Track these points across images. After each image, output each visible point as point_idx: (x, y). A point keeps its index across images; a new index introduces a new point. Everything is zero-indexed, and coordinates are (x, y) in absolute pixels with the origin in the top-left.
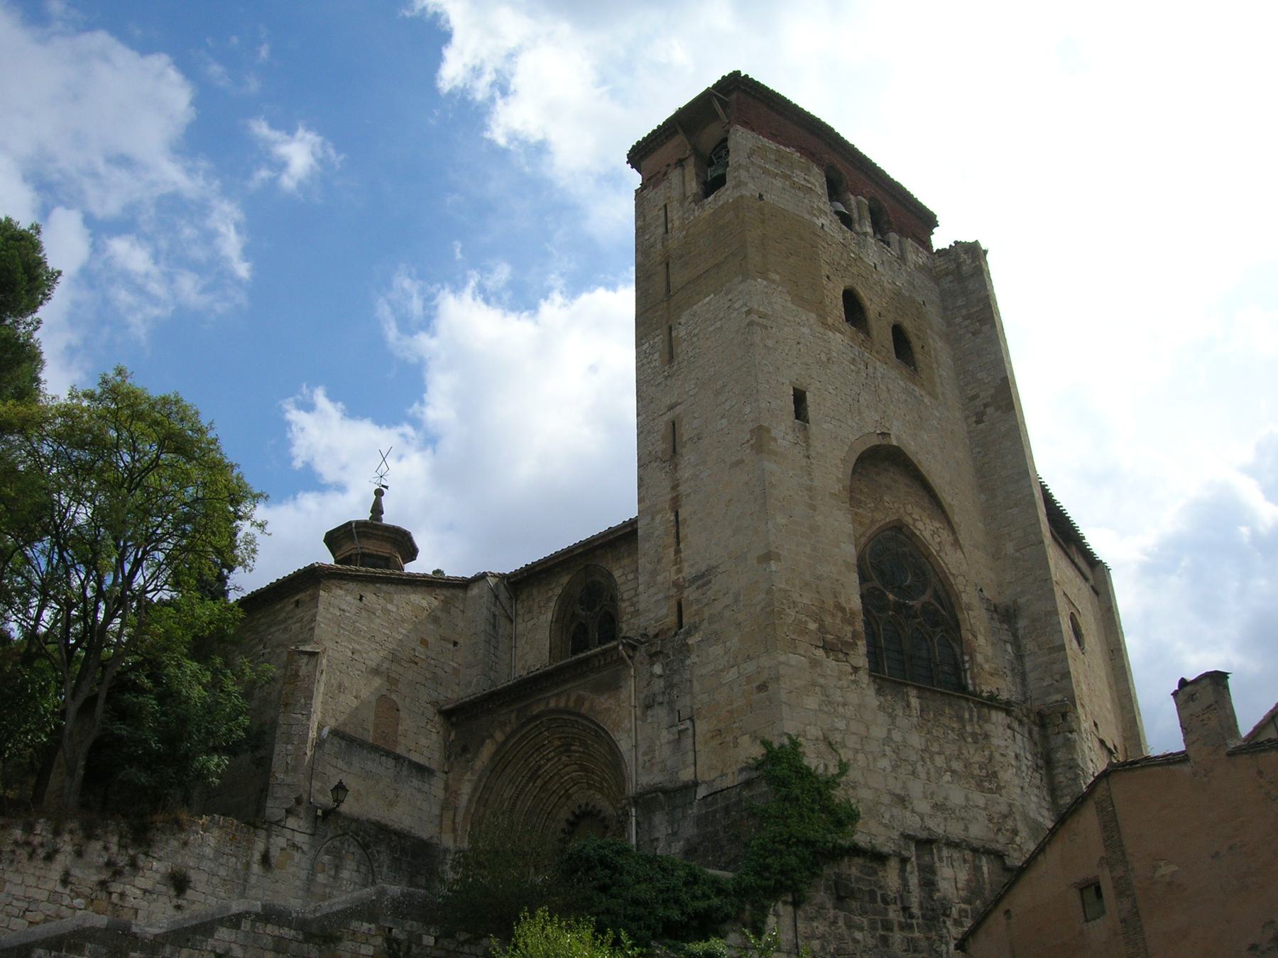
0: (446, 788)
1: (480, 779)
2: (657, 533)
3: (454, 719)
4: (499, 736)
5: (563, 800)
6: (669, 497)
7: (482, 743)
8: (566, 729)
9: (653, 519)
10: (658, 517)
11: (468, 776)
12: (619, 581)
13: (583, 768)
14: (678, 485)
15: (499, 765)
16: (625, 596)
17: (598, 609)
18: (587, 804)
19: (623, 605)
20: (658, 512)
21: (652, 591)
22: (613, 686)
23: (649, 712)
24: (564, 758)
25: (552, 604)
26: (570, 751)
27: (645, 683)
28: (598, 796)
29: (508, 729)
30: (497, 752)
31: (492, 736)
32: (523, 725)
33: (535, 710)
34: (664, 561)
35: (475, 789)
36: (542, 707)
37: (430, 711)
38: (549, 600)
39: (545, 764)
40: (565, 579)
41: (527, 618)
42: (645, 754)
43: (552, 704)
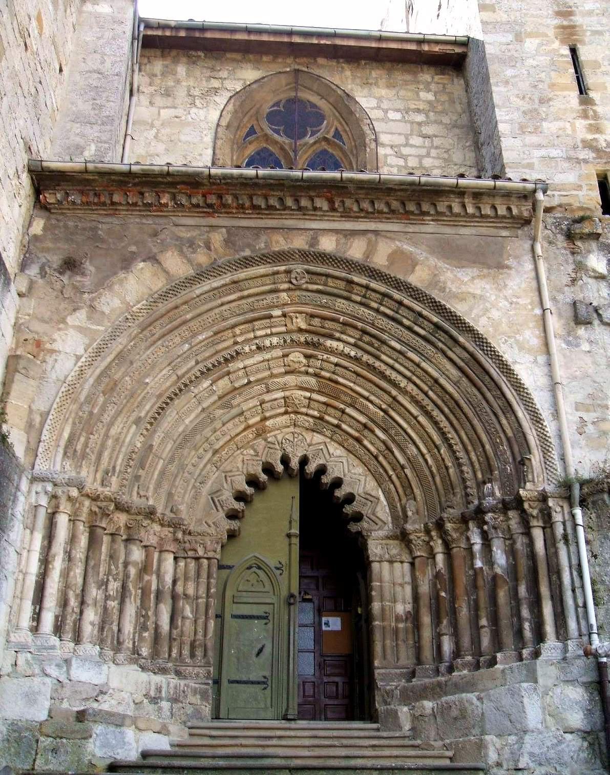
0: (17, 327)
1: (113, 337)
2: (531, 62)
3: (50, 197)
4: (177, 265)
5: (250, 434)
6: (557, 21)
7: (127, 263)
8: (341, 304)
9: (519, 38)
10: (530, 44)
11: (79, 318)
12: (374, 114)
13: (329, 387)
14: (571, 14)
15: (163, 316)
16: (383, 138)
17: (309, 139)
18: (304, 461)
19: (382, 151)
20: (530, 35)
21: (534, 139)
22: (491, 262)
23: (581, 331)
24: (297, 357)
25: (221, 100)
26: (316, 346)
27: (566, 280)
28: (336, 450)
29: (202, 258)
30: (164, 296)
31: (153, 259)
32: (247, 262)
33: (280, 243)
34: (557, 105)
35: (99, 352)
36: (299, 243)
37: (22, 159)
38: (216, 91)
39: (252, 354)
40: (250, 74)
41: (159, 101)
42: (578, 406)
43: (327, 244)
